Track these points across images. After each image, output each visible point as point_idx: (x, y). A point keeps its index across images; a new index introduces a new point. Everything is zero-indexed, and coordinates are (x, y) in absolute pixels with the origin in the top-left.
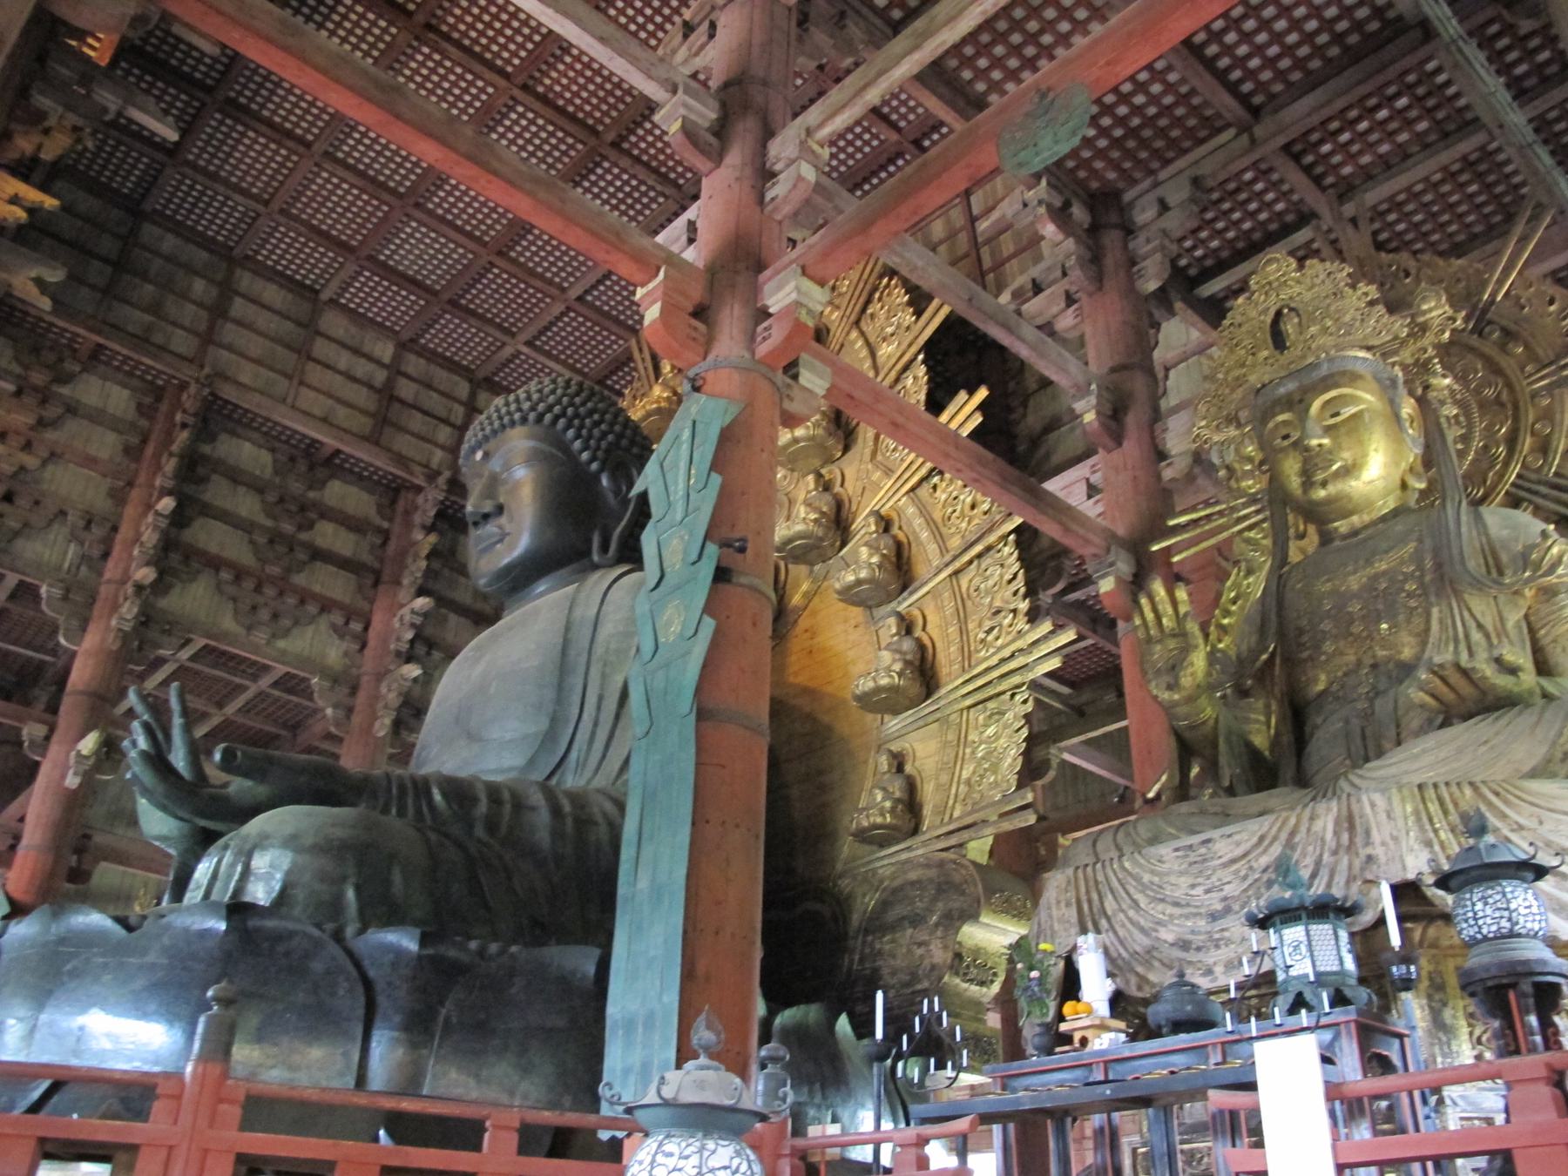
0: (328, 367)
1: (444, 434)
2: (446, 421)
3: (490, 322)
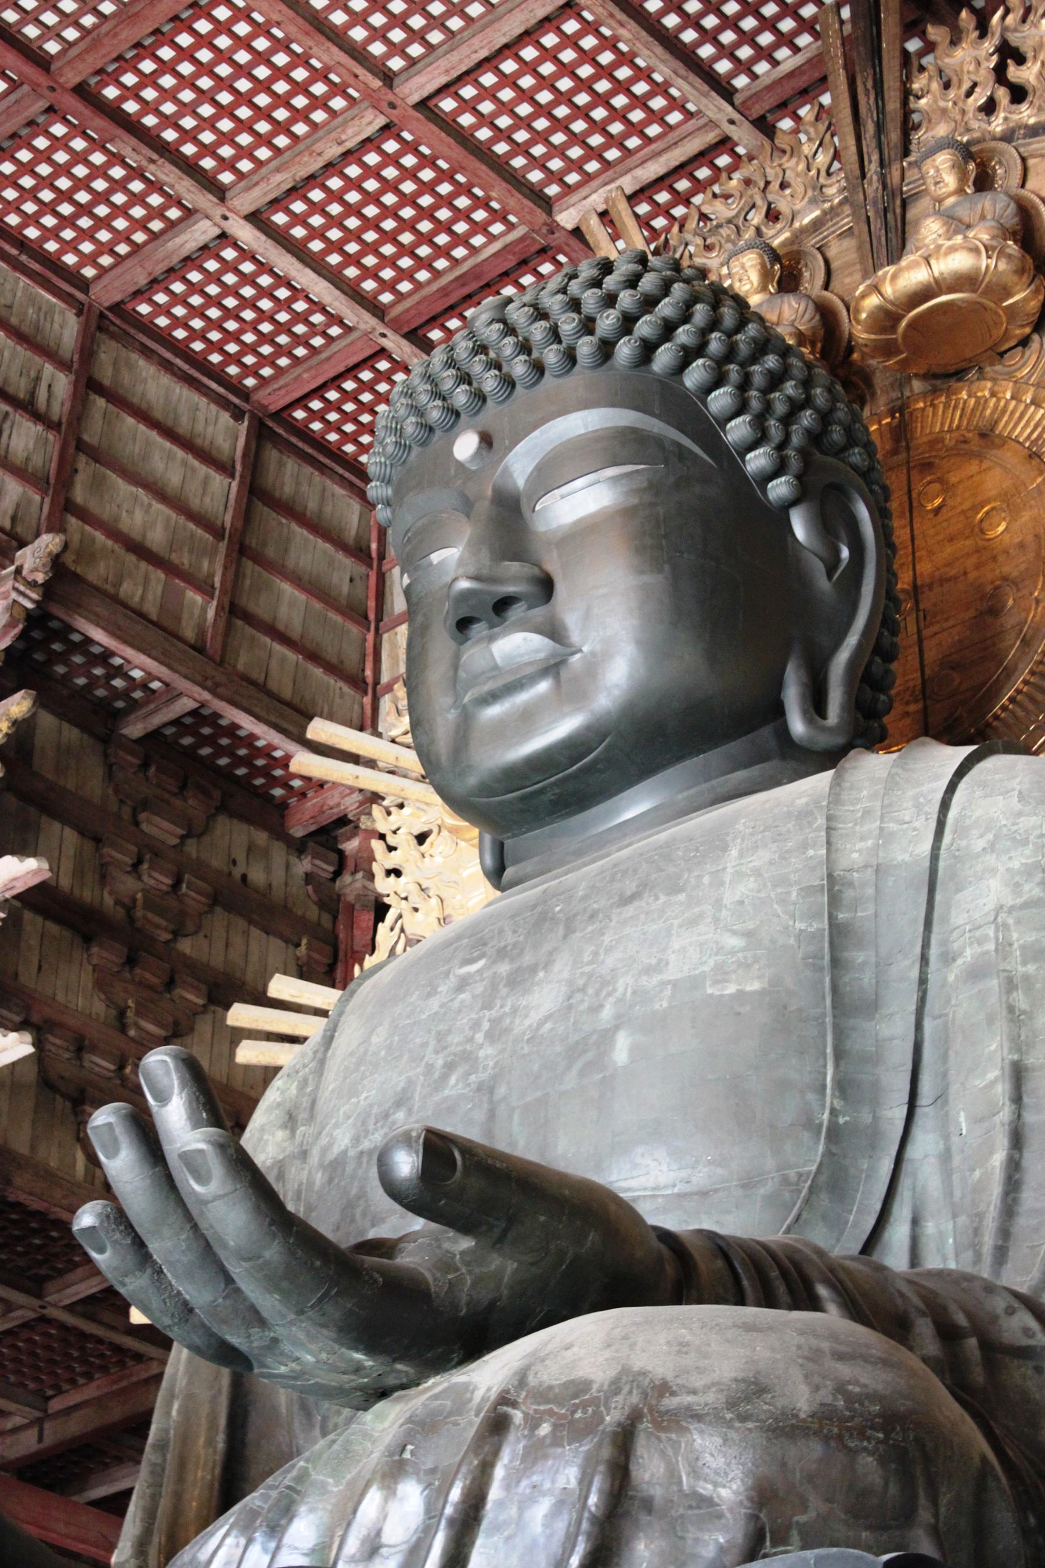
2: (28, 407)
3: (169, 152)
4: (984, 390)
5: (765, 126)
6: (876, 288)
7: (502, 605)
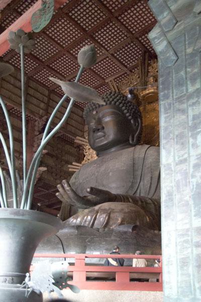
0: (8, 82)
1: (42, 105)
2: (43, 102)
3: (58, 73)
4: (155, 104)
5: (131, 71)
6: (142, 93)
7: (98, 130)
